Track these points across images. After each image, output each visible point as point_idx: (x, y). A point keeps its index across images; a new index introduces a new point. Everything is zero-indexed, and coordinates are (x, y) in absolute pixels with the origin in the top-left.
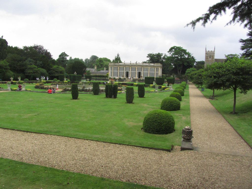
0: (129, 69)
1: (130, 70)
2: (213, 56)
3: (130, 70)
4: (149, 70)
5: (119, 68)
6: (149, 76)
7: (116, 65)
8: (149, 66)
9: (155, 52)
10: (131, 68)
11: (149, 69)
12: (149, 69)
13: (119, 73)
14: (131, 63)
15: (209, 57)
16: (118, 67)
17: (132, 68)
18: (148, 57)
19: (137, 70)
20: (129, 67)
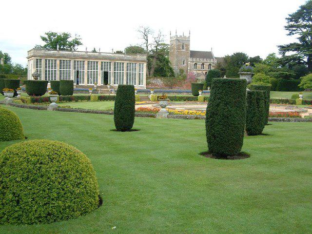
0: (84, 65)
1: (86, 66)
2: (188, 46)
3: (86, 66)
4: (125, 69)
5: (58, 62)
6: (58, 79)
7: (51, 56)
8: (126, 60)
9: (60, 30)
10: (86, 63)
11: (125, 65)
12: (125, 65)
13: (58, 73)
14: (100, 53)
15: (181, 48)
16: (56, 59)
17: (102, 62)
18: (44, 39)
19: (99, 66)
20: (84, 60)
